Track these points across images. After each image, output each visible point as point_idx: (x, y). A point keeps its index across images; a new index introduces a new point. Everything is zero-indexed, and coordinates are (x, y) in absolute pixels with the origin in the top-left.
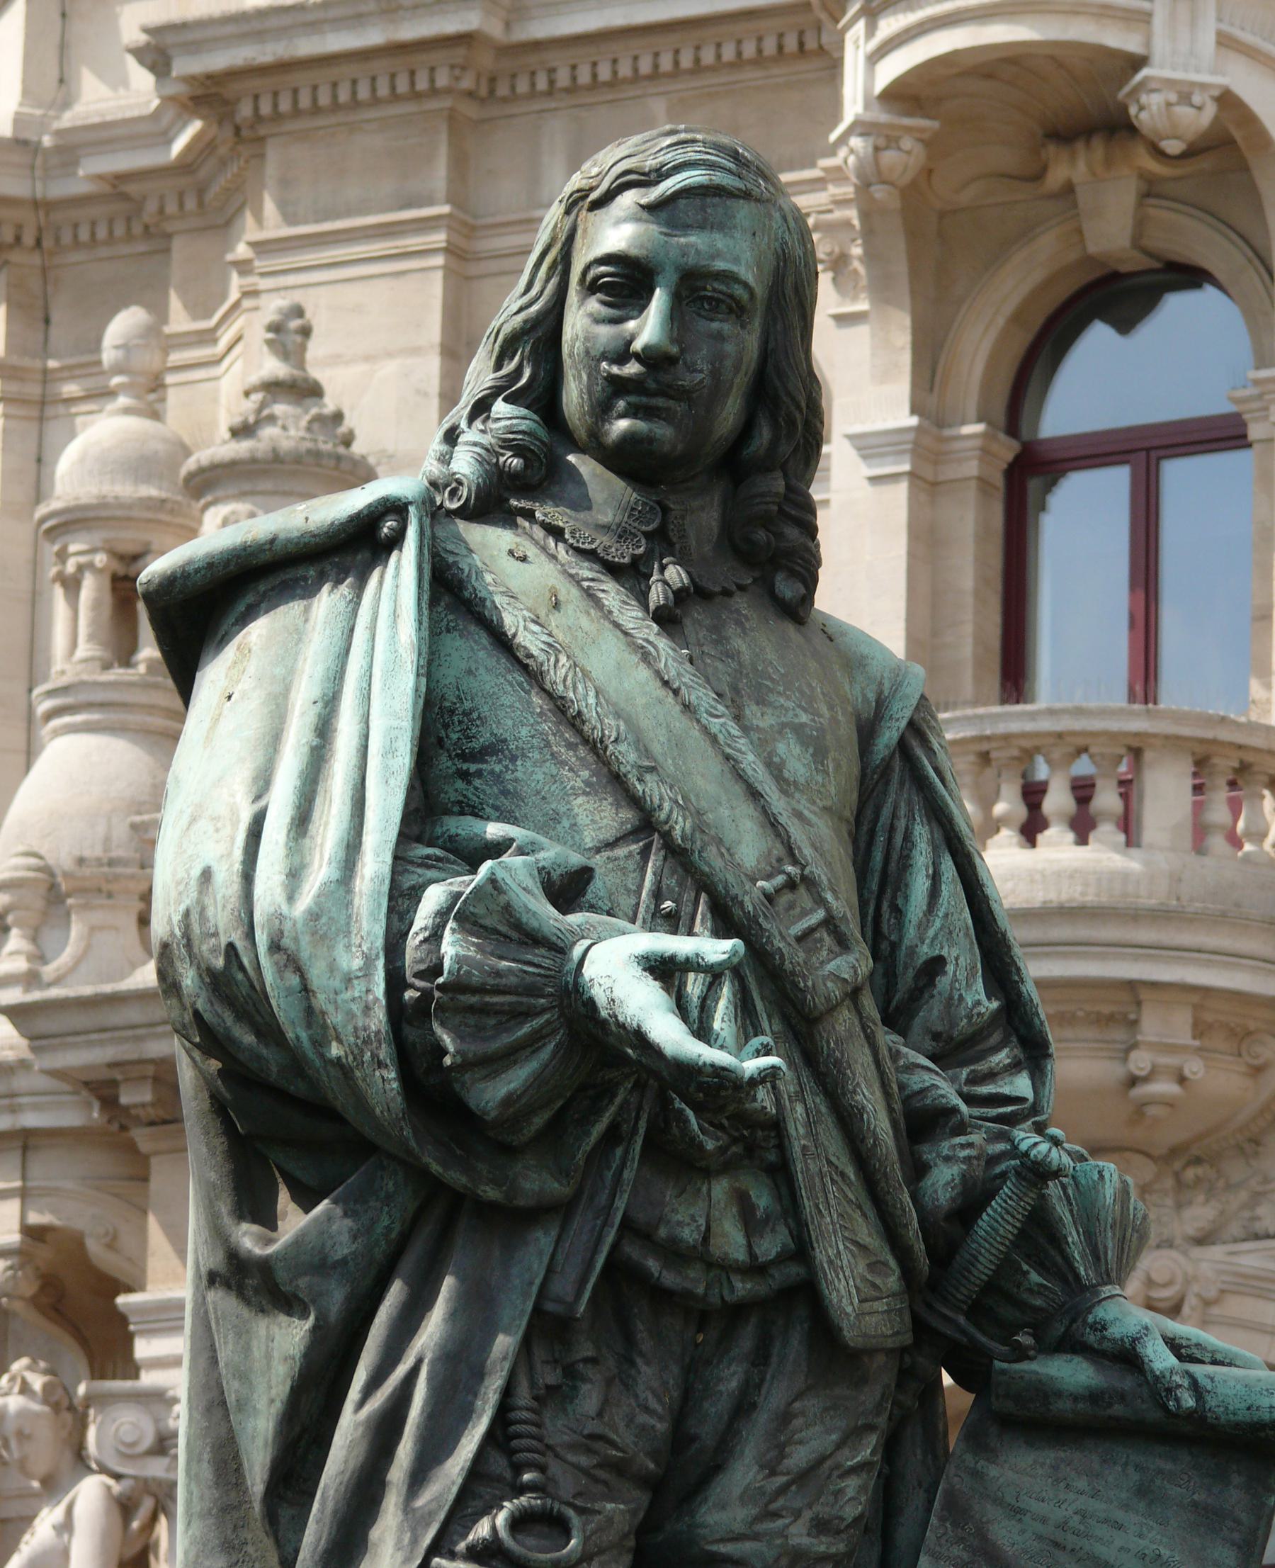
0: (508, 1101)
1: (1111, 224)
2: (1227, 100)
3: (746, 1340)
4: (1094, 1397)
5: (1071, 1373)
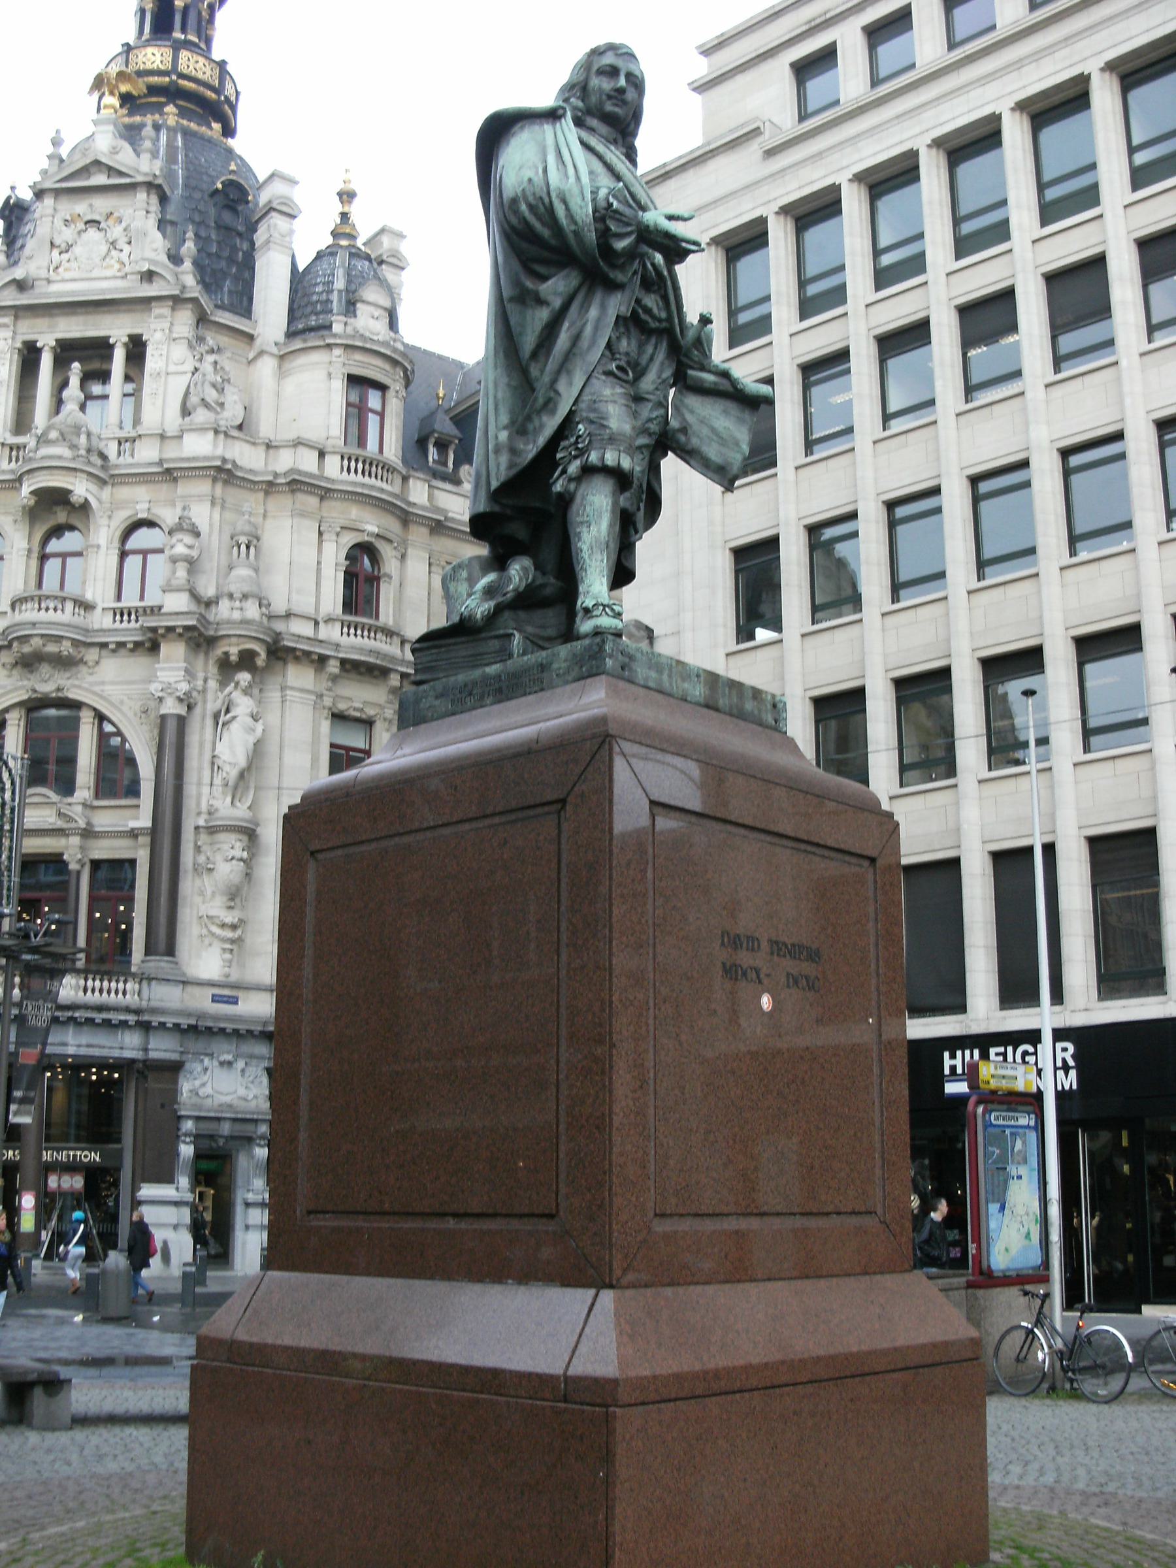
0: (624, 248)
1: (61, 517)
2: (86, 499)
3: (653, 341)
4: (715, 384)
5: (709, 378)
